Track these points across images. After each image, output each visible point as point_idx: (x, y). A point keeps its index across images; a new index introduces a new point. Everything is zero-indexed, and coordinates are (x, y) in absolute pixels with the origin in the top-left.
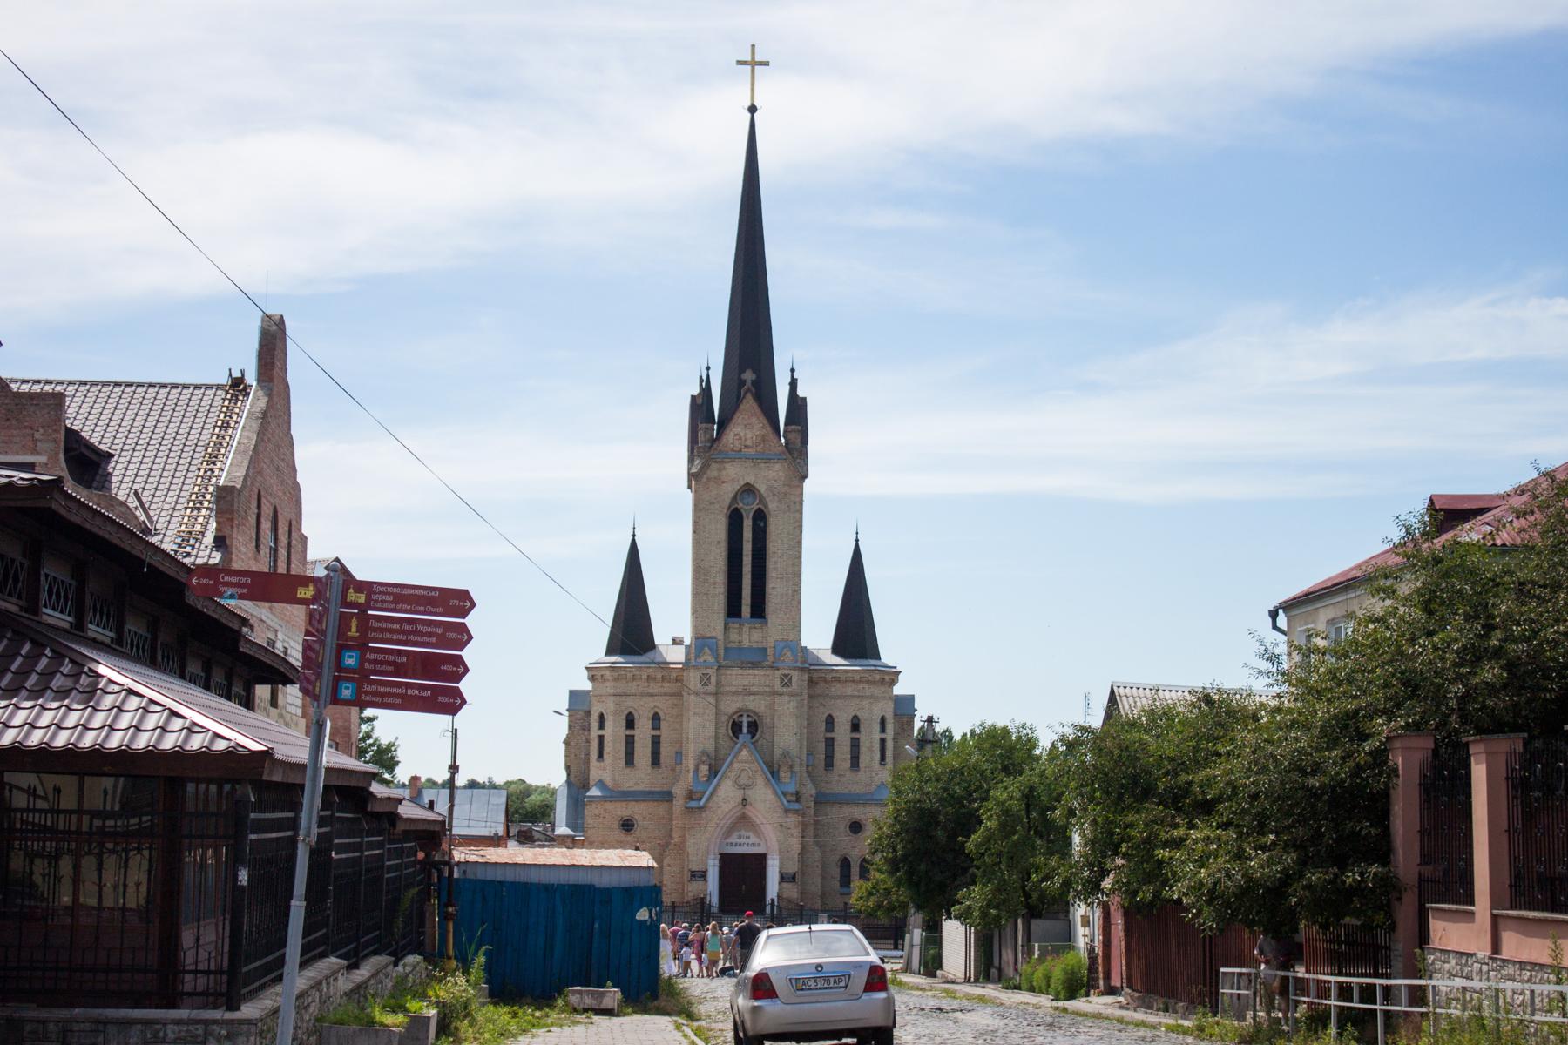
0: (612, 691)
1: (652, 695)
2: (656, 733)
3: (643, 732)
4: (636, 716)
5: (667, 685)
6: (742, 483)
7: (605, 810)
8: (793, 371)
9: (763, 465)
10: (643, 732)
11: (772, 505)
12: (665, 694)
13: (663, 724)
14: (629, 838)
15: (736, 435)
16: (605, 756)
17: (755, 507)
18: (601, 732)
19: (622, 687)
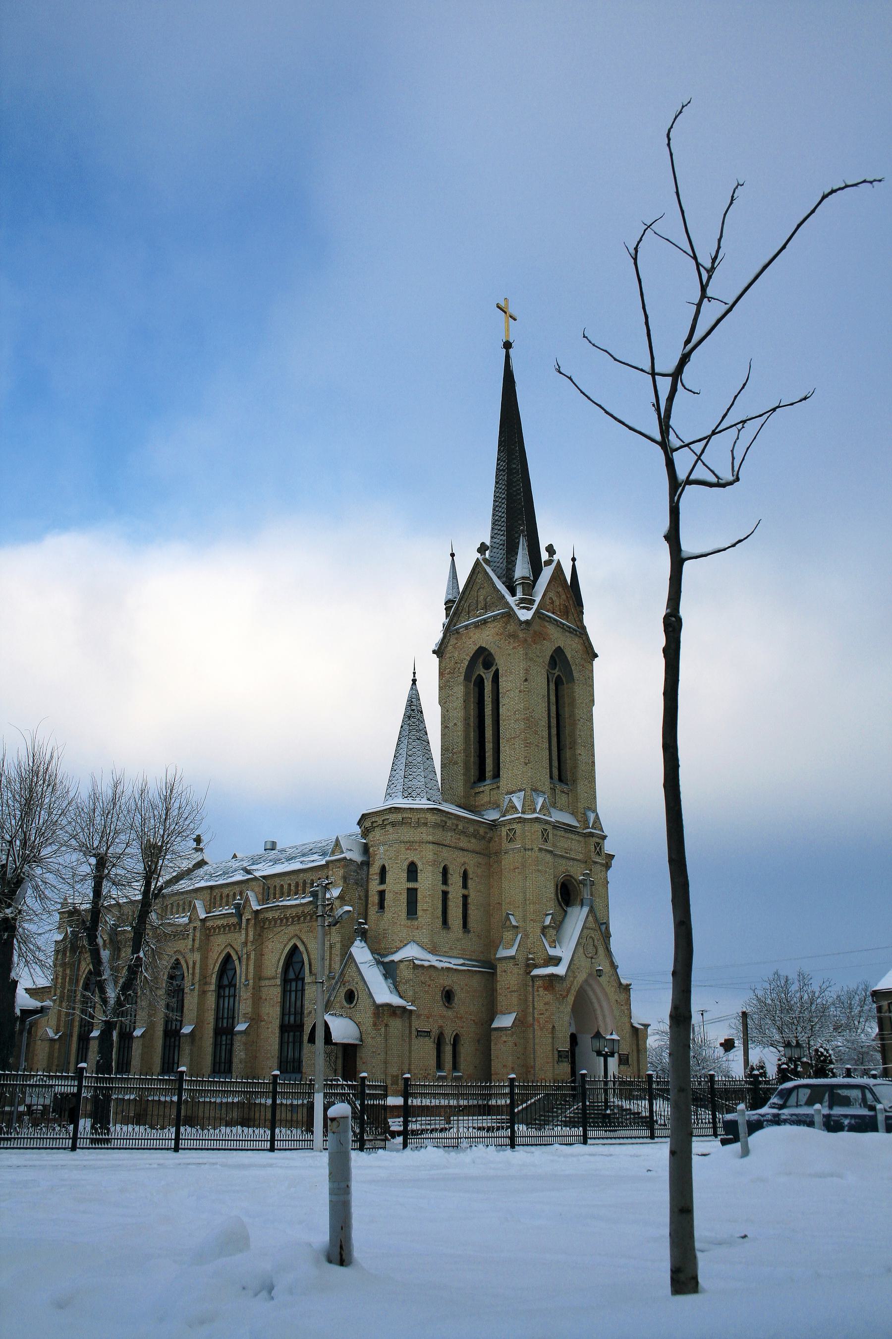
0: (430, 838)
1: (462, 849)
2: (465, 892)
3: (456, 891)
4: (451, 871)
5: (473, 840)
6: (556, 646)
7: (430, 977)
8: (574, 559)
9: (567, 634)
10: (456, 891)
11: (576, 675)
12: (474, 852)
13: (470, 883)
14: (450, 1013)
15: (551, 598)
16: (420, 913)
17: (557, 672)
18: (411, 885)
19: (439, 835)
